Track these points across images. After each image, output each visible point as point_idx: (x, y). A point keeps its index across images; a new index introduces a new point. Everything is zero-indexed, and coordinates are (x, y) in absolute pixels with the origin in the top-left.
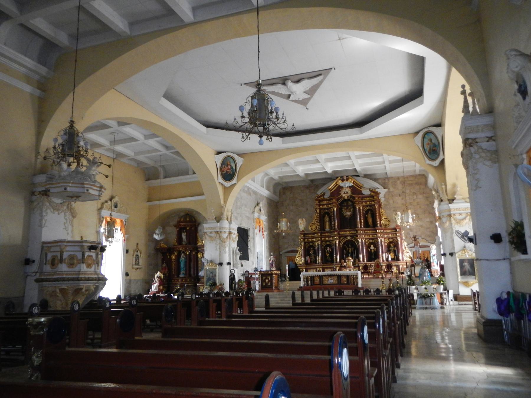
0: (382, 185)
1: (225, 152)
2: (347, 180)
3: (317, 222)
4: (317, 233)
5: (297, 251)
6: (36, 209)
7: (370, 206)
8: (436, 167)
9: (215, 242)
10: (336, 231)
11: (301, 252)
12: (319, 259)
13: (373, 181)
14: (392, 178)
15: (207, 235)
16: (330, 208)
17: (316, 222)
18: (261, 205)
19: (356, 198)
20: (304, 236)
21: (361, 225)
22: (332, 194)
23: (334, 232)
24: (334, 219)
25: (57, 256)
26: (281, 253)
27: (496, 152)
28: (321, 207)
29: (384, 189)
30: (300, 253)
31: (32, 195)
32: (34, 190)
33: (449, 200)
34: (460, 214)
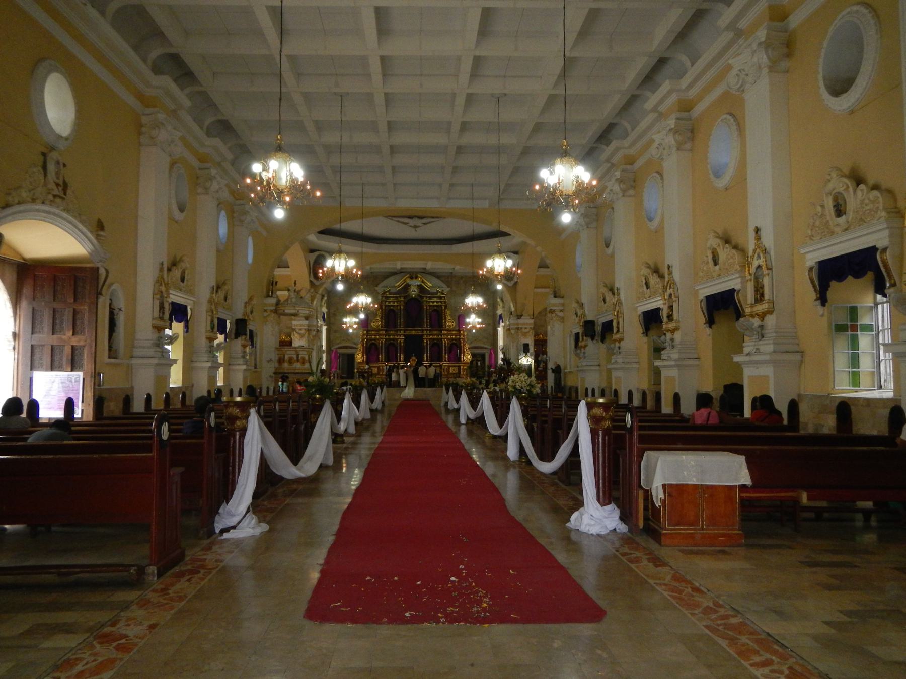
0: (444, 283)
1: (318, 251)
2: (416, 277)
3: (381, 318)
4: (382, 331)
5: (357, 349)
6: (267, 323)
7: (437, 306)
8: (509, 287)
9: (304, 339)
10: (402, 330)
11: (362, 350)
12: (381, 357)
13: (437, 279)
14: (455, 276)
15: (296, 331)
16: (397, 306)
17: (379, 319)
18: (326, 298)
19: (425, 298)
20: (367, 333)
21: (427, 325)
22: (399, 292)
23: (400, 330)
24: (400, 317)
25: (292, 357)
26: (332, 348)
27: (563, 318)
28: (387, 303)
29: (448, 287)
30: (360, 350)
31: (264, 312)
32: (265, 308)
33: (517, 316)
34: (526, 329)
